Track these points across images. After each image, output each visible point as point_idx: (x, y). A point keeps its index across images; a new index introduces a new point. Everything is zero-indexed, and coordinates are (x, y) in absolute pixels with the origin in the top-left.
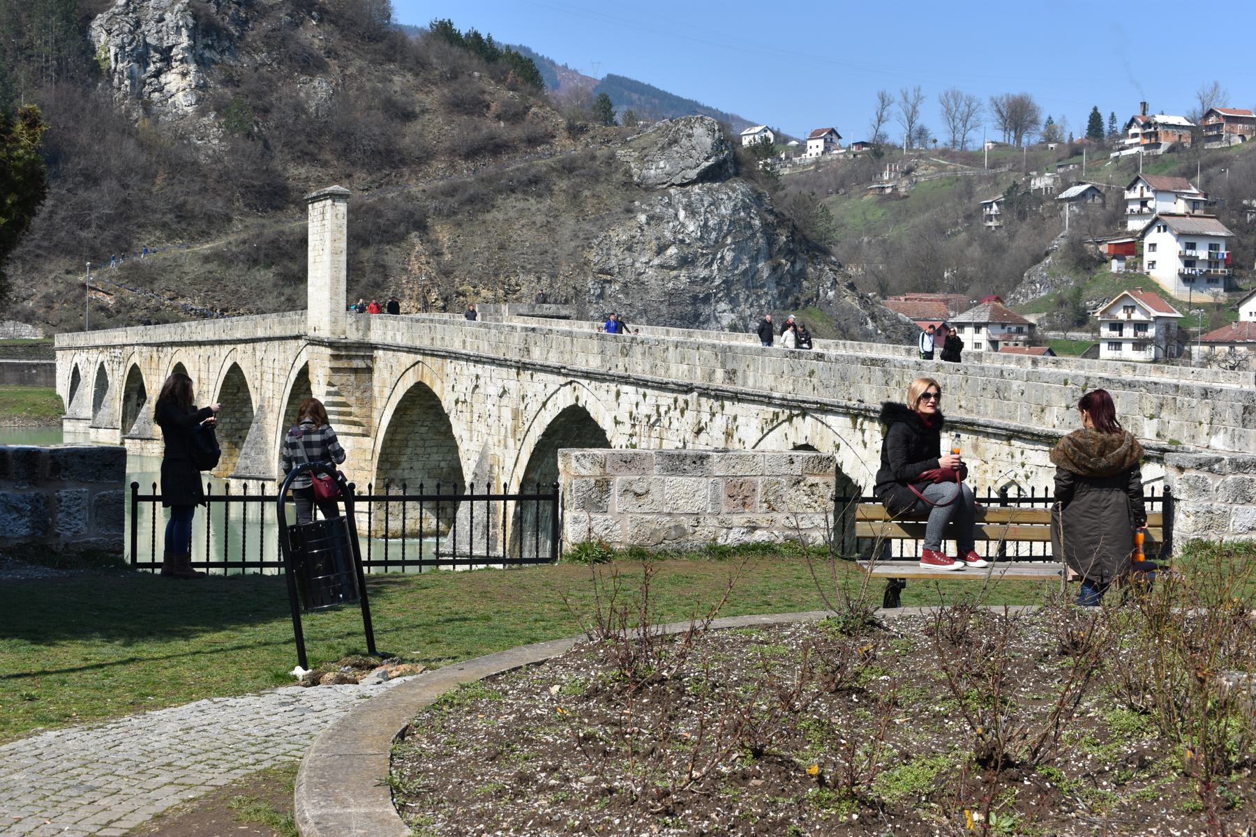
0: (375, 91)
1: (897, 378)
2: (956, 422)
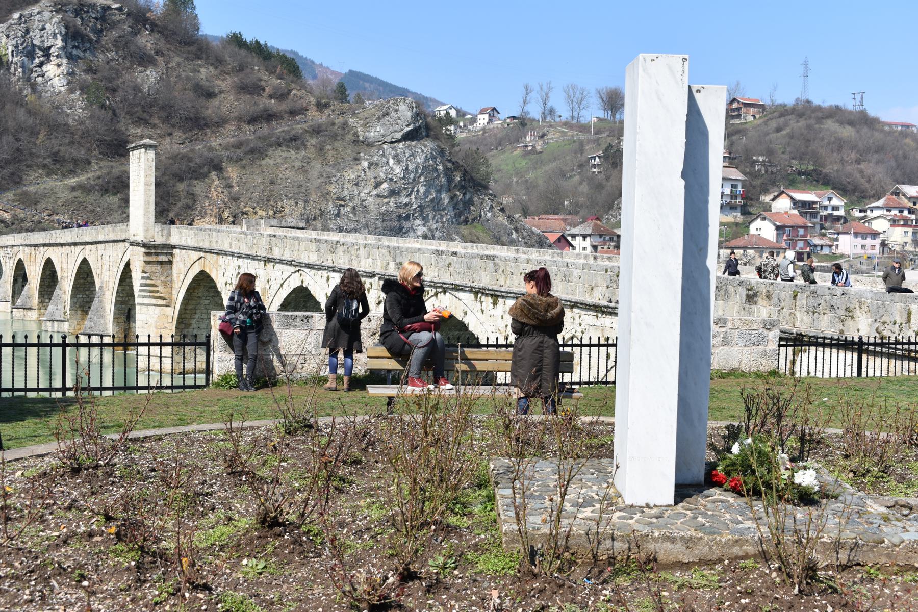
0: (188, 79)
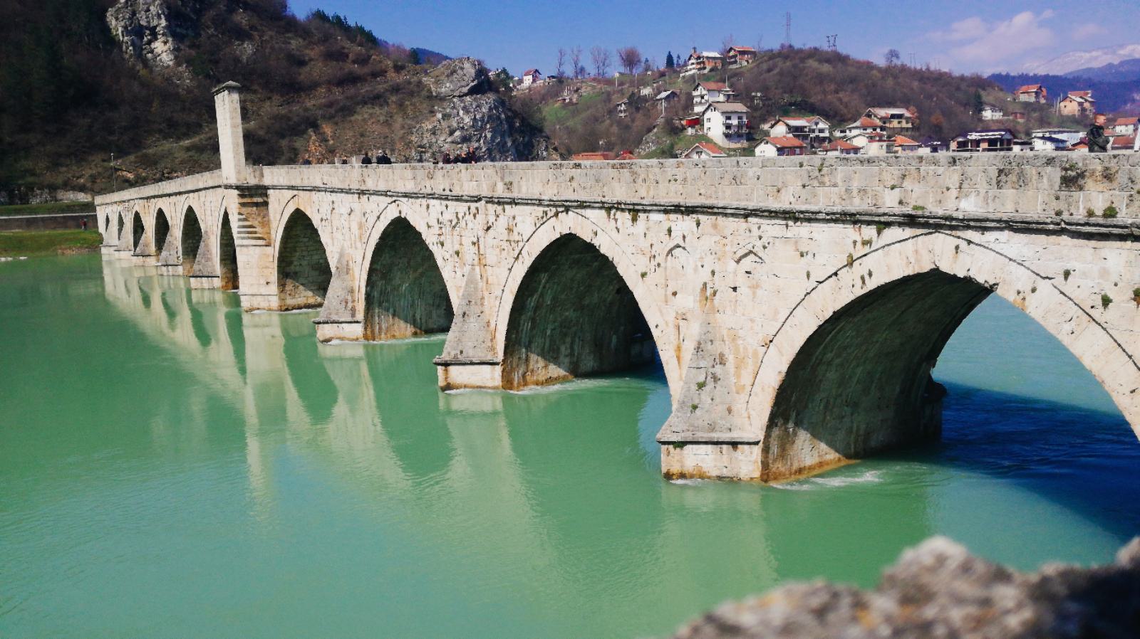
1: (642, 176)
2: (697, 207)
